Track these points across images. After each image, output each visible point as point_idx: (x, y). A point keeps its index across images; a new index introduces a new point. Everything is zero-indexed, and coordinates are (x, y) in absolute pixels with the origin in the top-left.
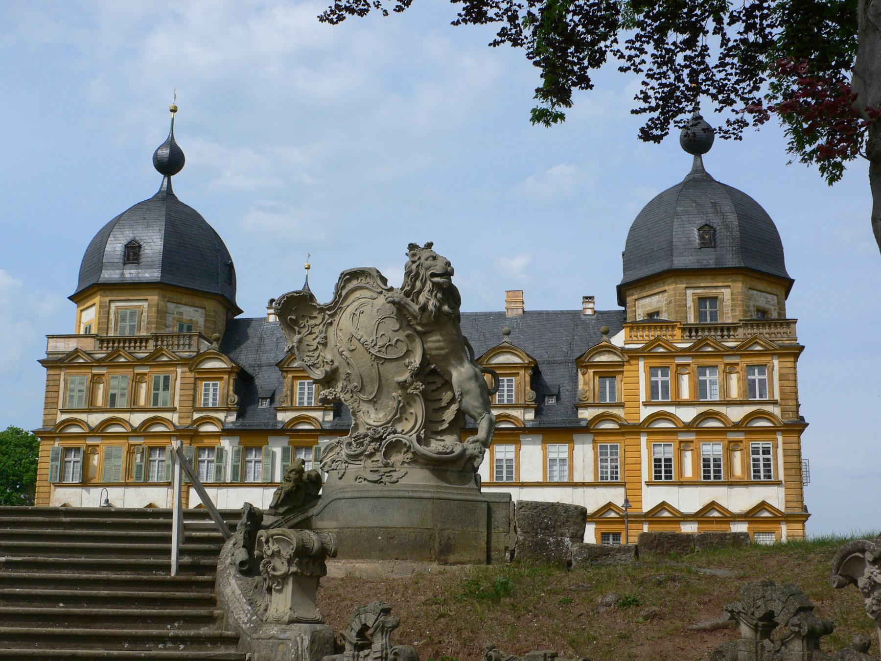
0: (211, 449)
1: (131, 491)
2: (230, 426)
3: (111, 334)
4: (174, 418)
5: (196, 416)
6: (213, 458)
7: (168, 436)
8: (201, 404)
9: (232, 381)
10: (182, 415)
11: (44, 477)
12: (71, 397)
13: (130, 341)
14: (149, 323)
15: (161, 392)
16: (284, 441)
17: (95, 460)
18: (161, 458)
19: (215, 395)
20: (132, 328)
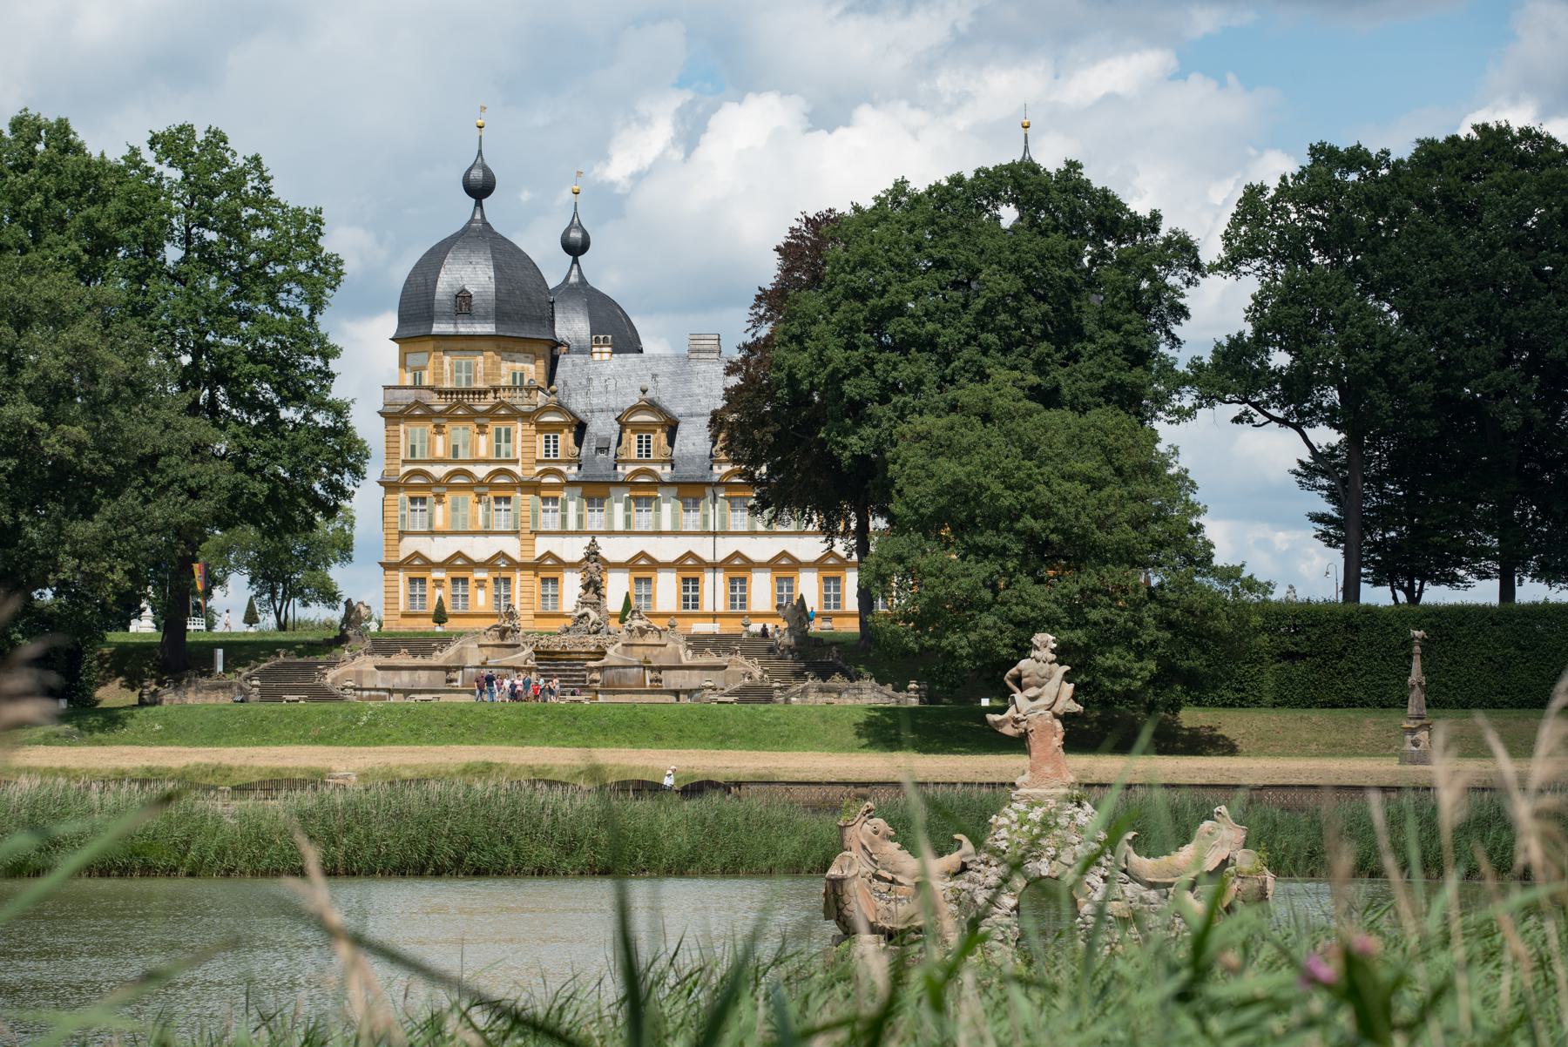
1: (480, 540)
2: (572, 478)
3: (447, 385)
4: (517, 469)
5: (538, 468)
6: (558, 507)
7: (512, 487)
8: (540, 455)
9: (571, 435)
11: (392, 526)
12: (413, 447)
13: (468, 393)
14: (485, 375)
15: (503, 444)
17: (439, 511)
18: (508, 507)
19: (555, 446)
20: (468, 379)
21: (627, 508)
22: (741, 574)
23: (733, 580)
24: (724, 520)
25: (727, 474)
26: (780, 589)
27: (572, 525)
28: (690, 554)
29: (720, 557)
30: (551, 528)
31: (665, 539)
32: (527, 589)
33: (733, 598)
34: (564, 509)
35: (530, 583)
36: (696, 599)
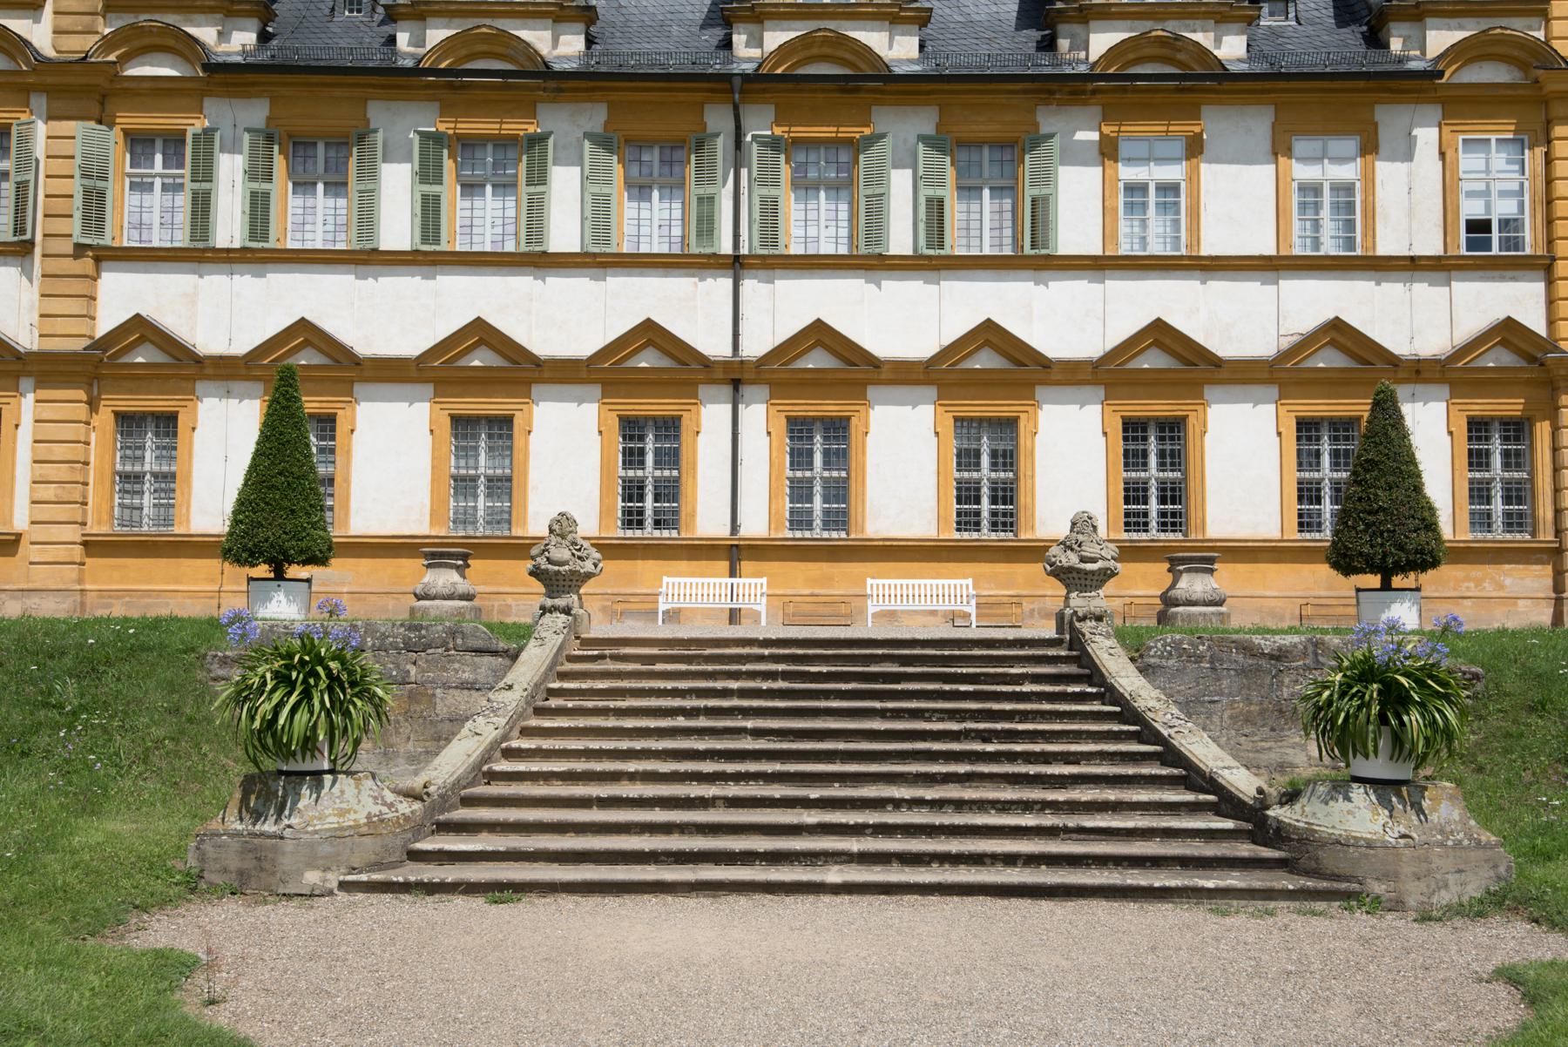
0: (174, 141)
10: (66, 22)
16: (421, 119)
21: (428, 173)
22: (831, 408)
23: (799, 429)
24: (771, 210)
25: (784, 50)
26: (967, 459)
27: (229, 229)
28: (650, 333)
29: (756, 345)
30: (157, 240)
31: (560, 286)
32: (59, 451)
33: (800, 491)
34: (204, 171)
35: (67, 432)
36: (669, 491)
